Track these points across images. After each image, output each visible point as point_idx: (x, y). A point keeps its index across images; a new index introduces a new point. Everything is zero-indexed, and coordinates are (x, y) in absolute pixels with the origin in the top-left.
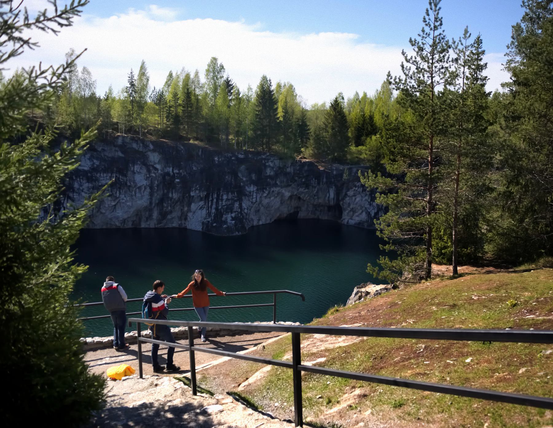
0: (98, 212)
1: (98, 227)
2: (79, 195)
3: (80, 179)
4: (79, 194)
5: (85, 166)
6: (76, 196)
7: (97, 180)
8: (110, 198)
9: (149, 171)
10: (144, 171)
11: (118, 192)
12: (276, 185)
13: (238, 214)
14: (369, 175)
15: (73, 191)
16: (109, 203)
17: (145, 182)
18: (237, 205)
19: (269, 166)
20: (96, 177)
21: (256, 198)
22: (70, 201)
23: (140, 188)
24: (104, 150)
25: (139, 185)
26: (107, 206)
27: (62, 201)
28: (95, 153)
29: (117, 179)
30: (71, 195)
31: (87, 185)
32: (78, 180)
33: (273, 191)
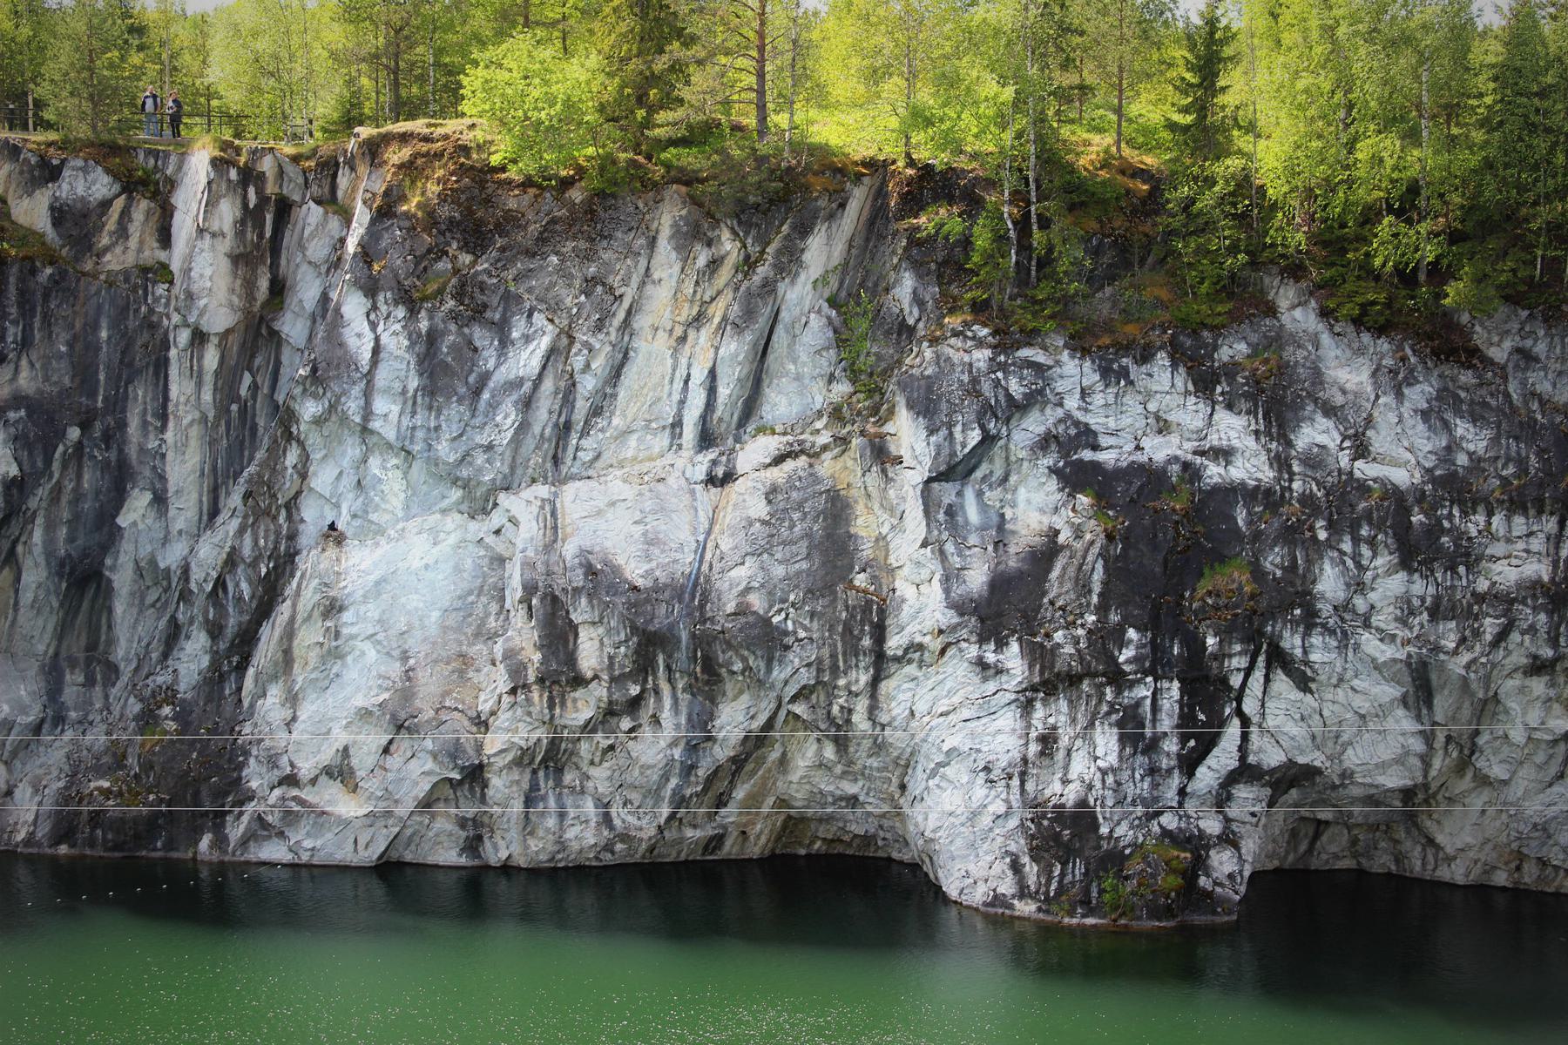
0: (1462, 766)
1: (1456, 873)
2: (1343, 647)
3: (1356, 540)
4: (1345, 641)
5: (1395, 463)
6: (1321, 651)
7: (1467, 556)
8: (1538, 686)
14: (780, 404)
15: (1310, 621)
16: (1534, 717)
20: (1459, 535)
22: (1281, 683)
24: (1526, 357)
26: (1518, 735)
27: (1236, 681)
28: (1467, 377)
30: (1292, 642)
31: (1396, 583)
32: (1347, 546)
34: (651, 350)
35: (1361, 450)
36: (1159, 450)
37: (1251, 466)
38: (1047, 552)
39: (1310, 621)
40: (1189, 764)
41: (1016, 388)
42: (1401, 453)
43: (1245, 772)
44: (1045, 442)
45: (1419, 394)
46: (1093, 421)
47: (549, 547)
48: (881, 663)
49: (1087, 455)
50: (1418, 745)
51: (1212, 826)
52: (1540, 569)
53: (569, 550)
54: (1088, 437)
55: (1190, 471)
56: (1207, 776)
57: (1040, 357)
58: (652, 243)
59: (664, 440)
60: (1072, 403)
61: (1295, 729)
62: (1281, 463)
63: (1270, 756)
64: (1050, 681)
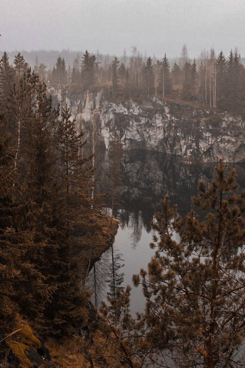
2: (132, 128)
9: (163, 118)
10: (161, 118)
11: (148, 129)
12: (227, 135)
13: (194, 150)
15: (129, 126)
17: (161, 125)
18: (194, 144)
19: (225, 121)
21: (212, 141)
23: (159, 127)
25: (158, 126)
27: (124, 131)
29: (148, 121)
30: (128, 128)
33: (224, 138)
34: (87, 102)
35: (134, 112)
36: (121, 111)
37: (127, 113)
38: (111, 120)
39: (129, 126)
40: (121, 138)
41: (109, 106)
42: (136, 112)
43: (125, 139)
44: (111, 111)
45: (138, 107)
46: (116, 109)
47: (81, 119)
48: (101, 129)
49: (115, 112)
50: (140, 137)
51: (123, 143)
52: (144, 122)
53: (82, 119)
54: (115, 110)
55: (123, 113)
56: (123, 139)
57: (112, 103)
58: (87, 94)
59: (88, 110)
60: (114, 107)
61: (130, 135)
62: (129, 113)
63: (128, 138)
64: (111, 131)
